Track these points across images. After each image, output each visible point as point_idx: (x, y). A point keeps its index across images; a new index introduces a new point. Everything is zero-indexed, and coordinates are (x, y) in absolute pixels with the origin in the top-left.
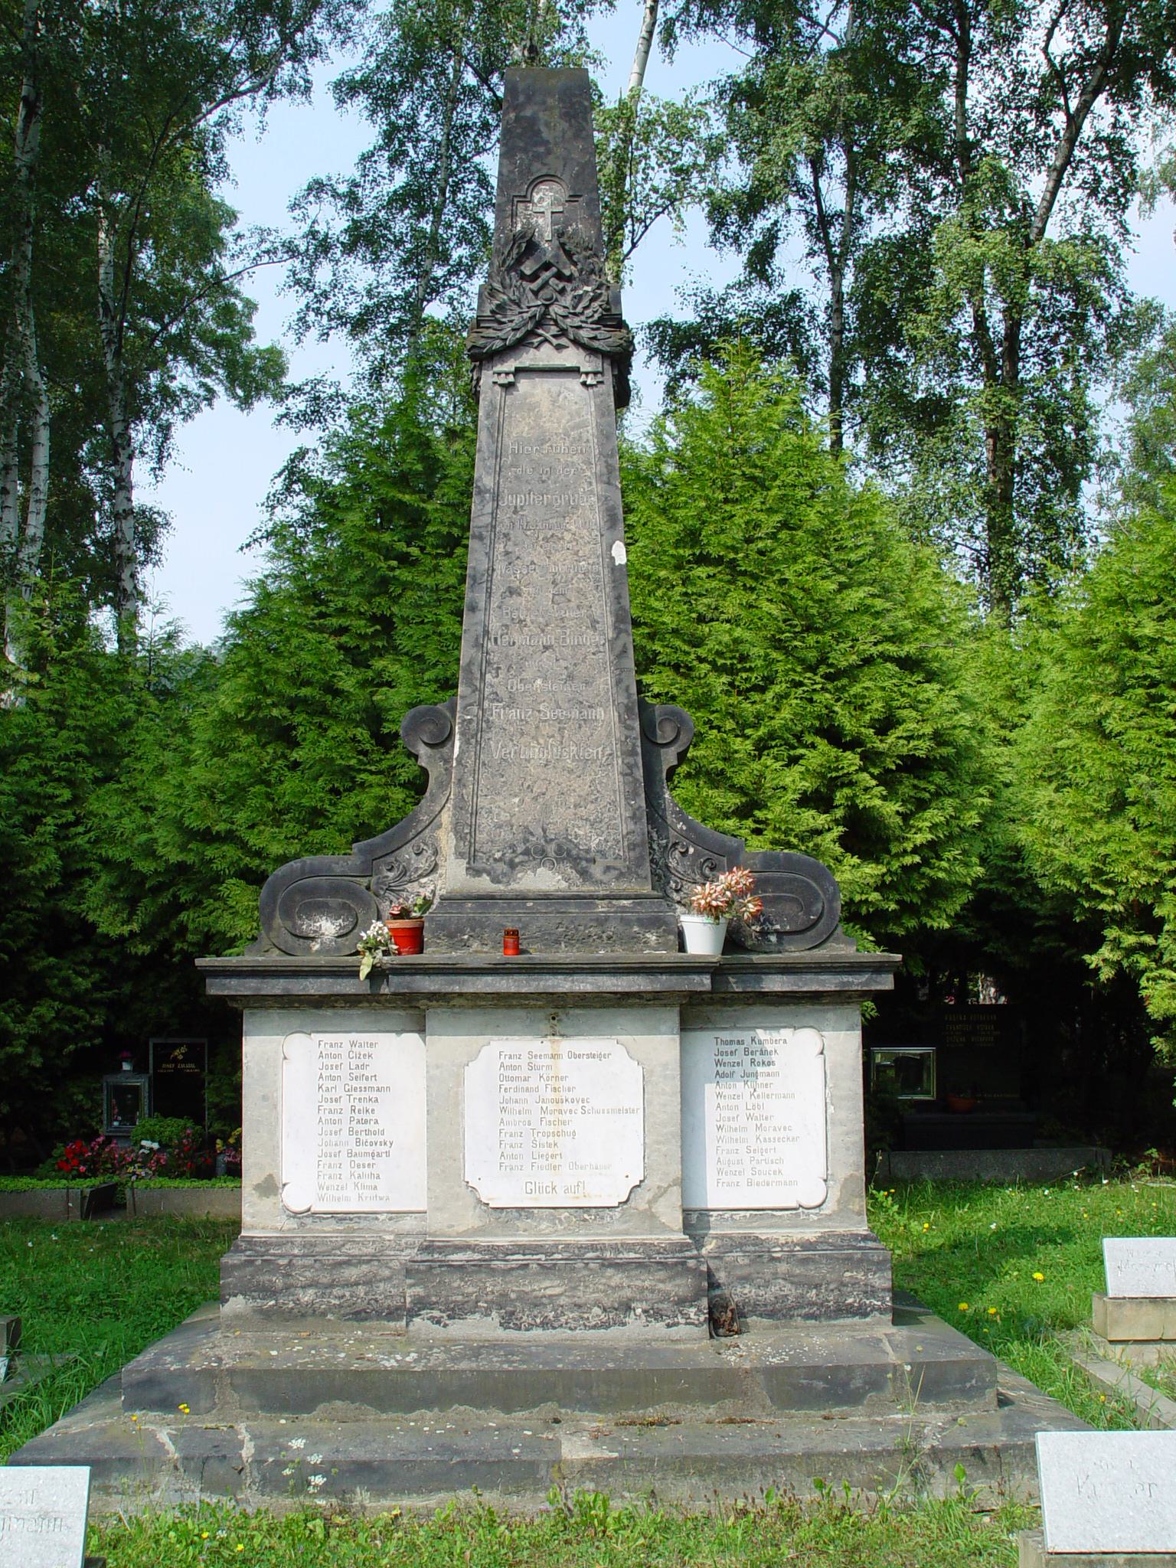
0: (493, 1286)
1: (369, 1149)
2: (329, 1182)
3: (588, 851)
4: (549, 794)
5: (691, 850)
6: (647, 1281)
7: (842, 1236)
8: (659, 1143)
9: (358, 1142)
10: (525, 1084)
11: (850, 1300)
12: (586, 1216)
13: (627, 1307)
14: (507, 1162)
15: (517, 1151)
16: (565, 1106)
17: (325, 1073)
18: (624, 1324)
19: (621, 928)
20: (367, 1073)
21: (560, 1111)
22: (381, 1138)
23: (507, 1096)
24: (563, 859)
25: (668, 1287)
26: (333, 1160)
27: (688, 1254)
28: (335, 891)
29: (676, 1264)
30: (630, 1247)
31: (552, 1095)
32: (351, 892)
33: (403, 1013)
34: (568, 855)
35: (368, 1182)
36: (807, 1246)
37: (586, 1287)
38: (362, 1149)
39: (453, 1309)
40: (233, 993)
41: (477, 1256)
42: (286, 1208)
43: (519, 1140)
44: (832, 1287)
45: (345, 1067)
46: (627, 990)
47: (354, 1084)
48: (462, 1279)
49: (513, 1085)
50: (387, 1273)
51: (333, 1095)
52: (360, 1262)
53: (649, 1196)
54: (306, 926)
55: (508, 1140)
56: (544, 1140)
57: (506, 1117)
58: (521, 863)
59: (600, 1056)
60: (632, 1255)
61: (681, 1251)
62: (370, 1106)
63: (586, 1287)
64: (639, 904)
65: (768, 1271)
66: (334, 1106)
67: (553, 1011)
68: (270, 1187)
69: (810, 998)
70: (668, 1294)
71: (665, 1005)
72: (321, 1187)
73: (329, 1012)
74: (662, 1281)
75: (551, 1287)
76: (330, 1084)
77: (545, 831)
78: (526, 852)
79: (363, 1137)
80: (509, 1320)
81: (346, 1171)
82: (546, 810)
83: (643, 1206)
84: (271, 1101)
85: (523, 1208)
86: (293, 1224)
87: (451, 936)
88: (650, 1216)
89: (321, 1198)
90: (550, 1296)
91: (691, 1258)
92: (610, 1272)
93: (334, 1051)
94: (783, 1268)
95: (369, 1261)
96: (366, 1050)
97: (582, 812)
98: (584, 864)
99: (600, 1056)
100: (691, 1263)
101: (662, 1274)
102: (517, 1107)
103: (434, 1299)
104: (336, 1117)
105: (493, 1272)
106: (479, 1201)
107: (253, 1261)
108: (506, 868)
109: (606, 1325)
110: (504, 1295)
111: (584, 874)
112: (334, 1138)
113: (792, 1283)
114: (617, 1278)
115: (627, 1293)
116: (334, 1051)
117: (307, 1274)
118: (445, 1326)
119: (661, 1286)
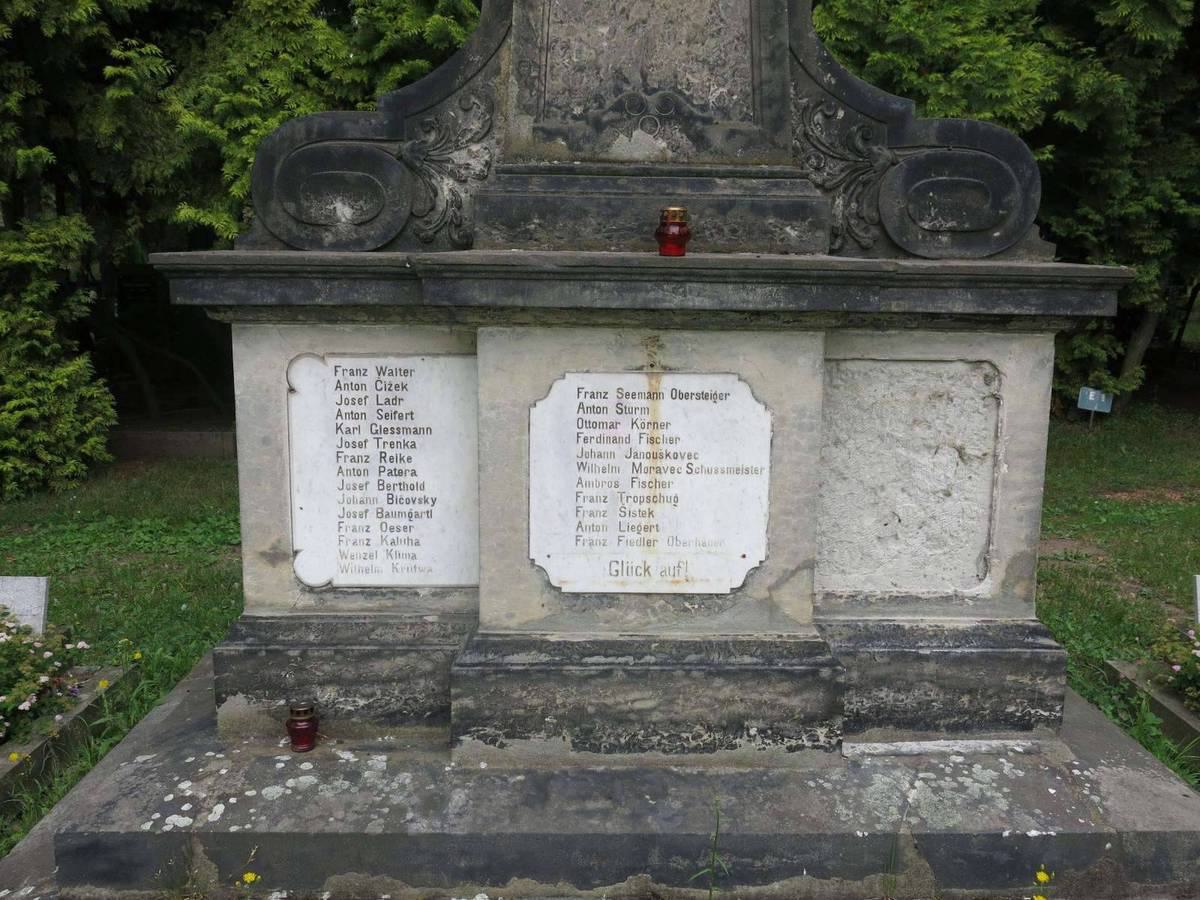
0: (564, 697)
1: (406, 508)
2: (353, 550)
3: (704, 108)
4: (652, 22)
5: (841, 114)
6: (767, 694)
7: (1006, 628)
8: (787, 513)
9: (391, 499)
10: (612, 433)
11: (1011, 709)
12: (687, 605)
13: (737, 726)
14: (586, 535)
15: (599, 521)
16: (666, 463)
17: (345, 409)
18: (733, 747)
19: (751, 218)
20: (401, 409)
21: (659, 470)
22: (418, 494)
23: (587, 448)
24: (669, 118)
25: (795, 702)
26: (358, 522)
27: (820, 659)
28: (354, 158)
29: (804, 674)
30: (743, 647)
31: (645, 447)
32: (372, 162)
33: (446, 329)
34: (673, 110)
35: (402, 548)
36: (962, 637)
37: (686, 700)
38: (396, 508)
39: (512, 726)
40: (208, 302)
41: (544, 658)
42: (299, 581)
43: (602, 507)
44: (990, 692)
45: (371, 401)
46: (761, 307)
47: (384, 423)
48: (523, 688)
49: (596, 433)
50: (428, 666)
51: (356, 437)
52: (394, 654)
53: (770, 581)
54: (315, 211)
55: (588, 506)
56: (636, 507)
57: (586, 476)
58: (612, 123)
59: (715, 397)
60: (747, 659)
61: (810, 655)
62: (406, 453)
63: (686, 700)
64: (776, 185)
65: (911, 671)
66: (358, 452)
67: (649, 332)
68: (281, 555)
69: (994, 323)
70: (792, 710)
71: (807, 329)
72: (343, 555)
73: (348, 328)
74: (786, 695)
75: (643, 699)
76: (350, 423)
77: (644, 76)
78: (618, 107)
79: (397, 493)
80: (585, 741)
81: (375, 534)
82: (647, 46)
83: (764, 594)
84: (277, 447)
85: (605, 595)
86: (308, 600)
87: (511, 226)
88: (770, 606)
89: (344, 570)
90: (640, 712)
91: (823, 665)
92: (718, 682)
93: (355, 380)
94: (930, 668)
95: (405, 653)
96: (399, 379)
97: (698, 50)
98: (699, 125)
99: (715, 397)
100: (825, 672)
101: (785, 686)
102: (601, 463)
103: (487, 713)
104: (361, 466)
105: (565, 680)
106: (549, 584)
107: (255, 653)
108: (589, 130)
109: (710, 748)
110: (579, 709)
111: (700, 140)
112: (358, 494)
113: (942, 687)
114: (727, 691)
115: (740, 708)
116: (355, 380)
117: (326, 668)
118: (502, 746)
119: (784, 700)
